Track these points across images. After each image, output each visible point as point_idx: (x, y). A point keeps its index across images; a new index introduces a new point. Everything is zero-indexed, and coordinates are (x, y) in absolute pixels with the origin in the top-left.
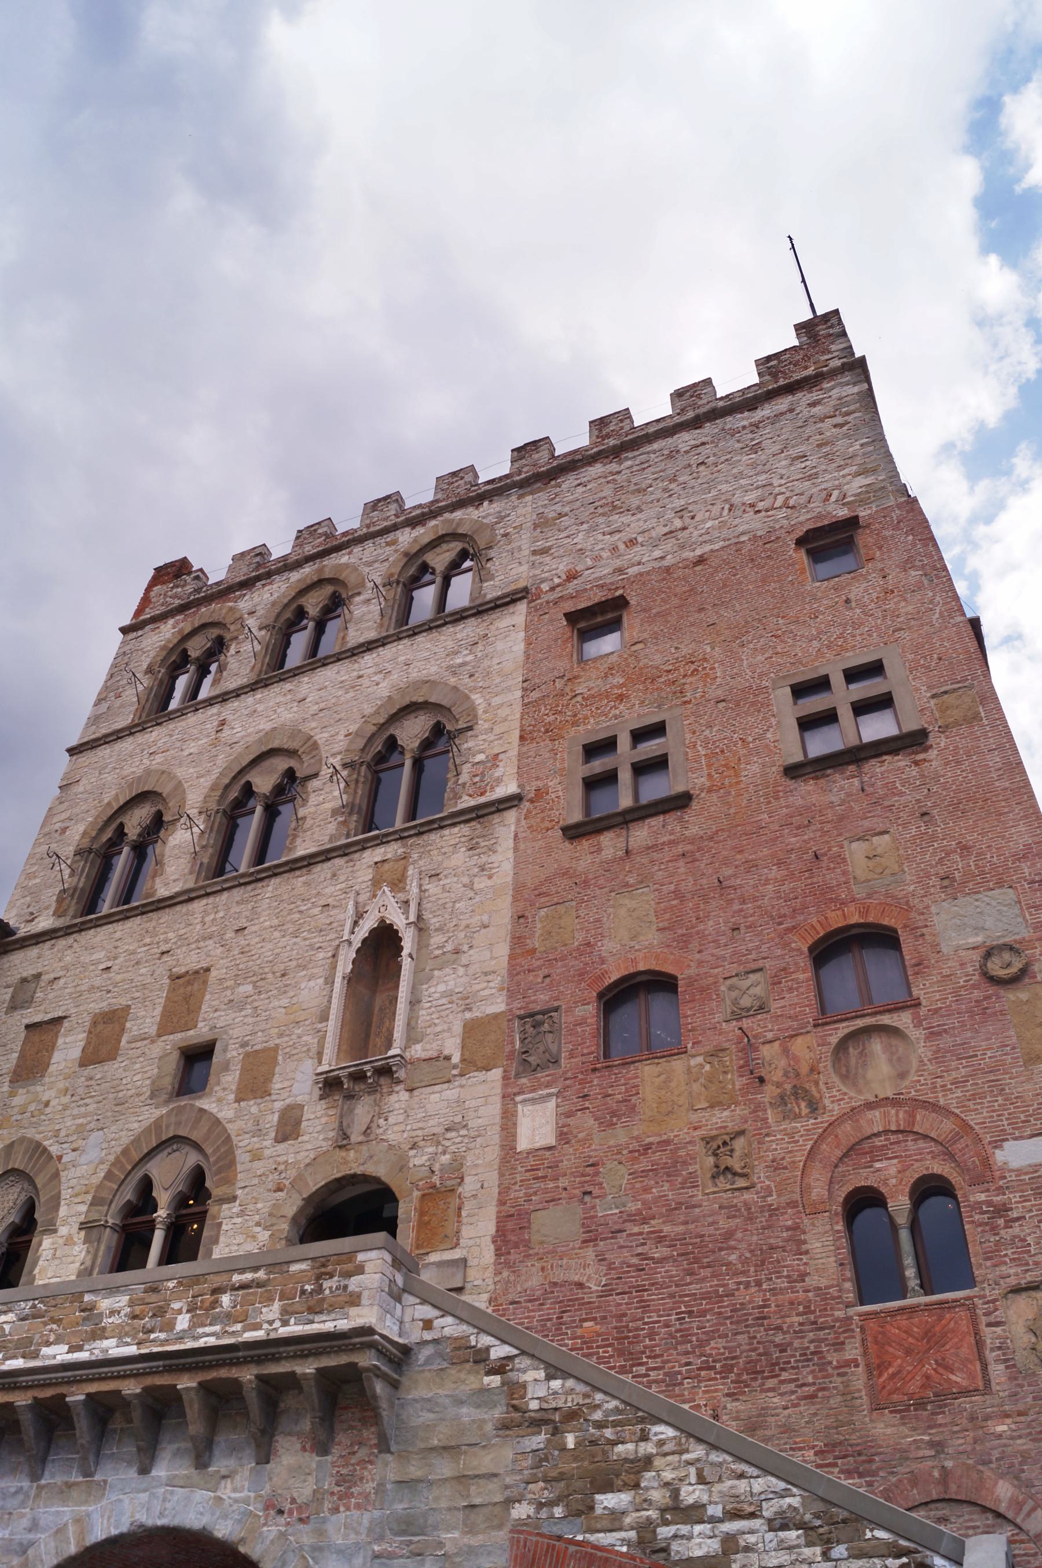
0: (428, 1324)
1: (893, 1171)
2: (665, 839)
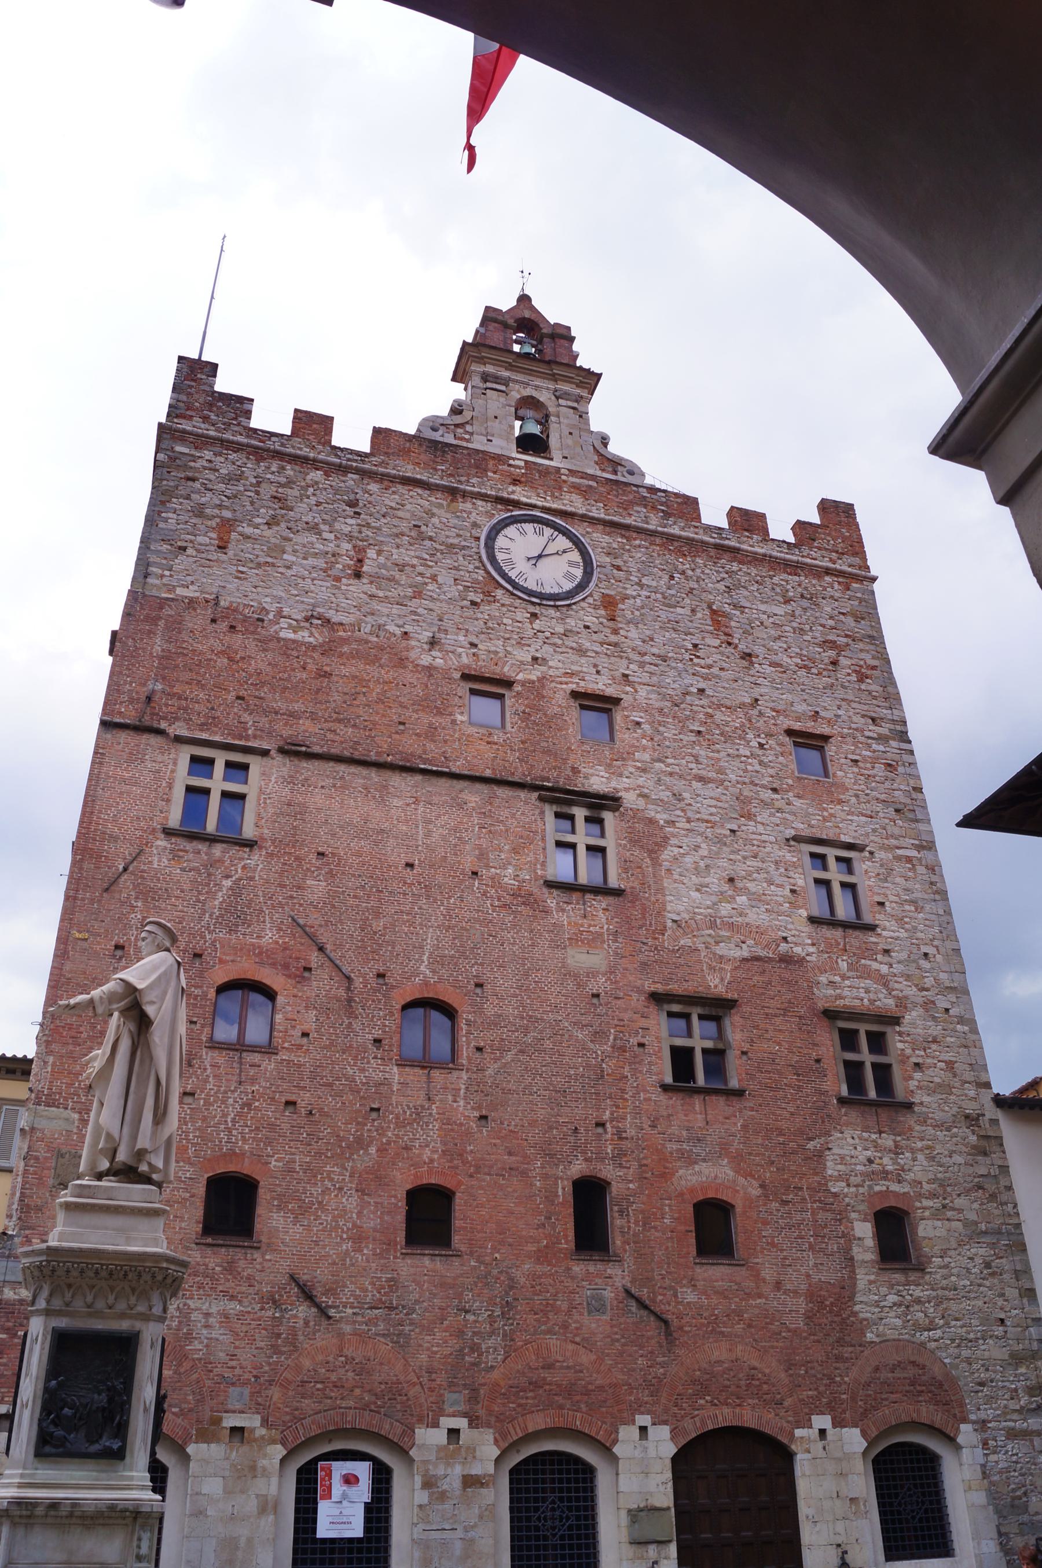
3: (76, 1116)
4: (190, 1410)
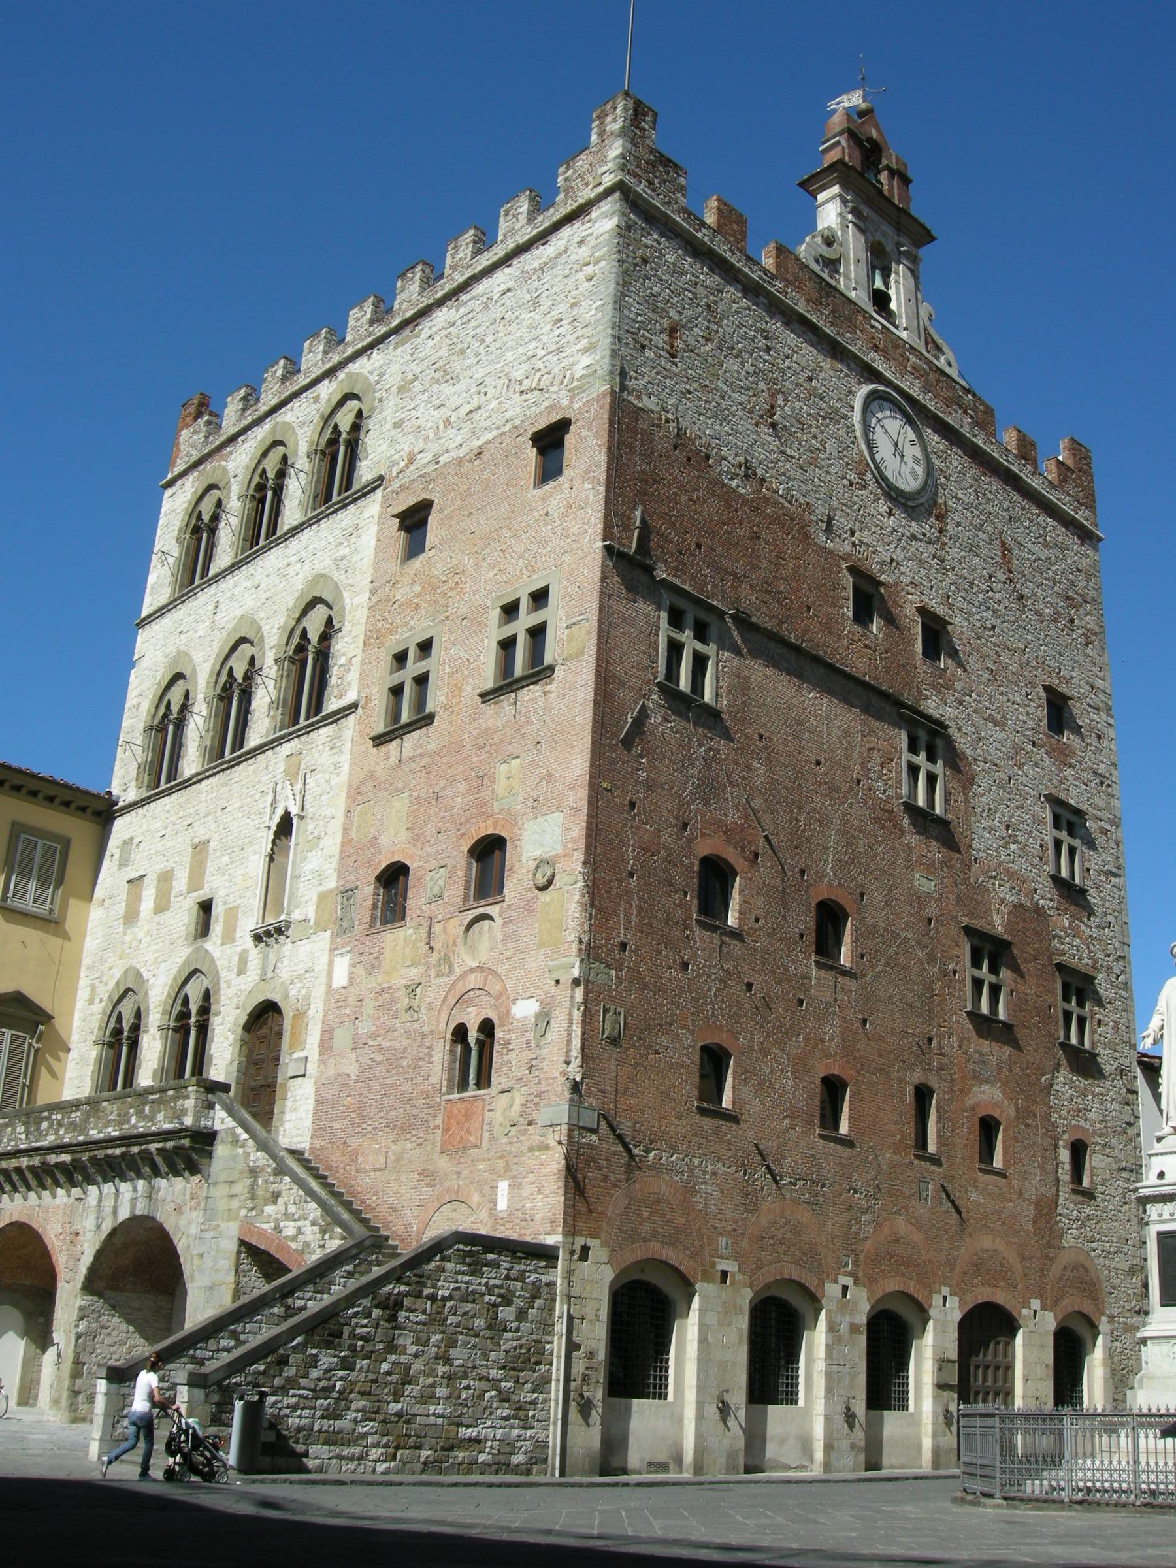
0: (223, 1120)
1: (473, 1015)
2: (418, 752)
3: (614, 972)
4: (697, 1254)
